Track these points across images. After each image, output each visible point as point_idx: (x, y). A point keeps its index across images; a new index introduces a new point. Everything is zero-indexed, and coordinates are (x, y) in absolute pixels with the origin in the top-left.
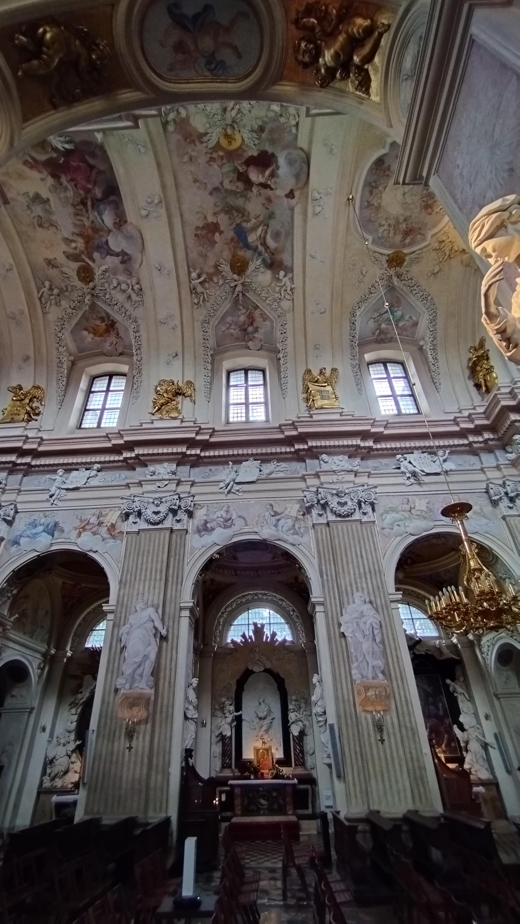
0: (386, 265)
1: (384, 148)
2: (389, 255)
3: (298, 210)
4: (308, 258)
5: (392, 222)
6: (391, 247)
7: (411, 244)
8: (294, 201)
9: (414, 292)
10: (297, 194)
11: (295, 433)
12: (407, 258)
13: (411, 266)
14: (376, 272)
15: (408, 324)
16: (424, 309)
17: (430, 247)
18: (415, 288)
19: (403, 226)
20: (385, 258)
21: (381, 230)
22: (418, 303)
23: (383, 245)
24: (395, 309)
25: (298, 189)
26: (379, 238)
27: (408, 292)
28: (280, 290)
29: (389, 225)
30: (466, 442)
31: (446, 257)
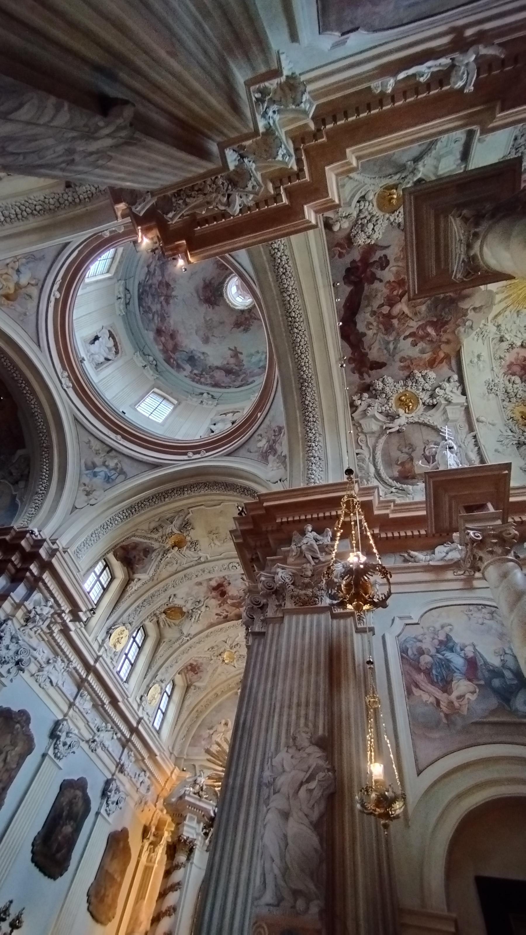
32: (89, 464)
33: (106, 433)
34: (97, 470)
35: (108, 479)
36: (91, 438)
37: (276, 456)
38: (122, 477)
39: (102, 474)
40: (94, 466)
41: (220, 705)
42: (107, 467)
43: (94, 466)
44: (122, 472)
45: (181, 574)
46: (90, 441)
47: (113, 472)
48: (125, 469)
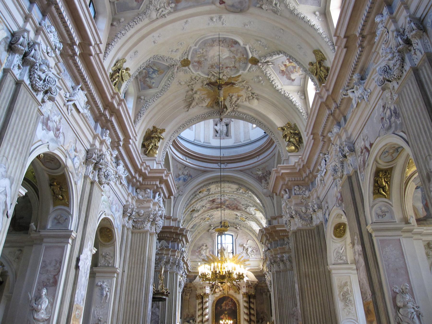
0: (182, 60)
1: (243, 44)
2: (187, 59)
3: (213, 7)
4: (185, 20)
5: (205, 54)
6: (191, 57)
7: (194, 66)
8: (218, 4)
9: (170, 80)
10: (223, 5)
11: (116, 105)
12: (187, 68)
13: (182, 71)
14: (178, 57)
15: (149, 83)
16: (161, 88)
17: (192, 74)
18: (172, 79)
19: (203, 59)
20: (185, 58)
21: (201, 50)
22: (163, 84)
23: (193, 53)
24: (156, 73)
25: (225, 6)
26: (196, 51)
27: (168, 76)
28: (163, 7)
29: (203, 53)
30: (133, 174)
31: (189, 84)
32: (177, 175)
33: (182, 158)
34: (180, 177)
35: (185, 180)
36: (178, 163)
37: (266, 182)
38: (190, 178)
39: (182, 178)
40: (179, 175)
41: (201, 237)
42: (184, 174)
43: (179, 175)
44: (190, 176)
45: (199, 201)
46: (177, 165)
47: (186, 176)
48: (191, 174)
